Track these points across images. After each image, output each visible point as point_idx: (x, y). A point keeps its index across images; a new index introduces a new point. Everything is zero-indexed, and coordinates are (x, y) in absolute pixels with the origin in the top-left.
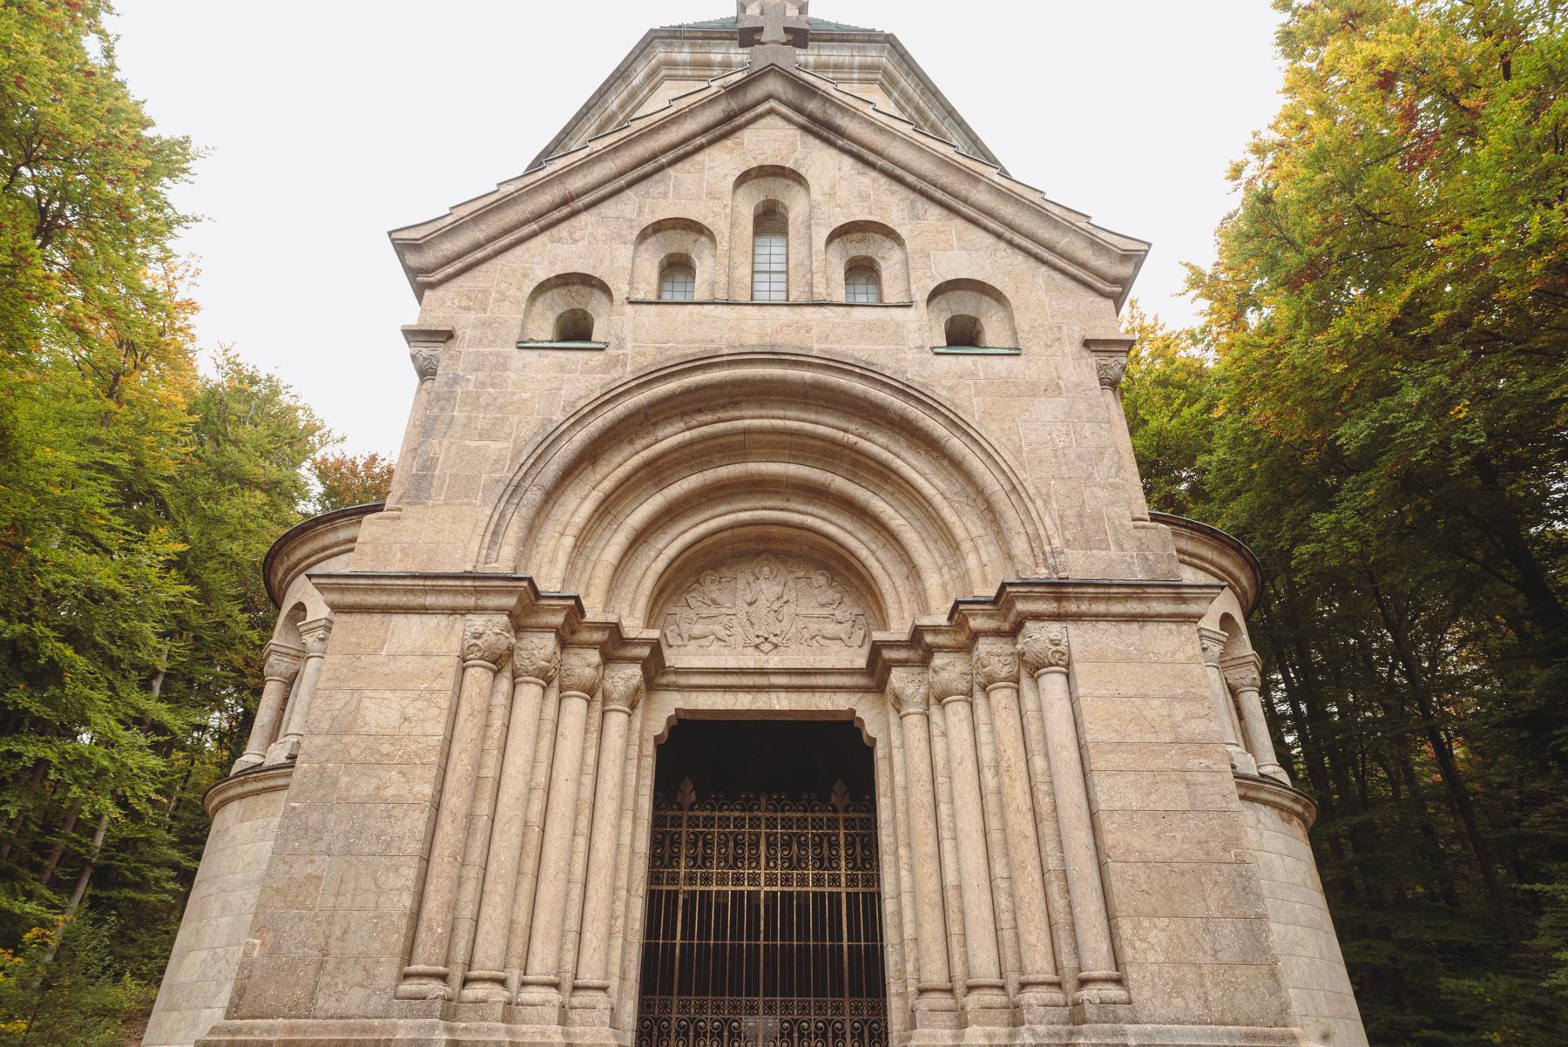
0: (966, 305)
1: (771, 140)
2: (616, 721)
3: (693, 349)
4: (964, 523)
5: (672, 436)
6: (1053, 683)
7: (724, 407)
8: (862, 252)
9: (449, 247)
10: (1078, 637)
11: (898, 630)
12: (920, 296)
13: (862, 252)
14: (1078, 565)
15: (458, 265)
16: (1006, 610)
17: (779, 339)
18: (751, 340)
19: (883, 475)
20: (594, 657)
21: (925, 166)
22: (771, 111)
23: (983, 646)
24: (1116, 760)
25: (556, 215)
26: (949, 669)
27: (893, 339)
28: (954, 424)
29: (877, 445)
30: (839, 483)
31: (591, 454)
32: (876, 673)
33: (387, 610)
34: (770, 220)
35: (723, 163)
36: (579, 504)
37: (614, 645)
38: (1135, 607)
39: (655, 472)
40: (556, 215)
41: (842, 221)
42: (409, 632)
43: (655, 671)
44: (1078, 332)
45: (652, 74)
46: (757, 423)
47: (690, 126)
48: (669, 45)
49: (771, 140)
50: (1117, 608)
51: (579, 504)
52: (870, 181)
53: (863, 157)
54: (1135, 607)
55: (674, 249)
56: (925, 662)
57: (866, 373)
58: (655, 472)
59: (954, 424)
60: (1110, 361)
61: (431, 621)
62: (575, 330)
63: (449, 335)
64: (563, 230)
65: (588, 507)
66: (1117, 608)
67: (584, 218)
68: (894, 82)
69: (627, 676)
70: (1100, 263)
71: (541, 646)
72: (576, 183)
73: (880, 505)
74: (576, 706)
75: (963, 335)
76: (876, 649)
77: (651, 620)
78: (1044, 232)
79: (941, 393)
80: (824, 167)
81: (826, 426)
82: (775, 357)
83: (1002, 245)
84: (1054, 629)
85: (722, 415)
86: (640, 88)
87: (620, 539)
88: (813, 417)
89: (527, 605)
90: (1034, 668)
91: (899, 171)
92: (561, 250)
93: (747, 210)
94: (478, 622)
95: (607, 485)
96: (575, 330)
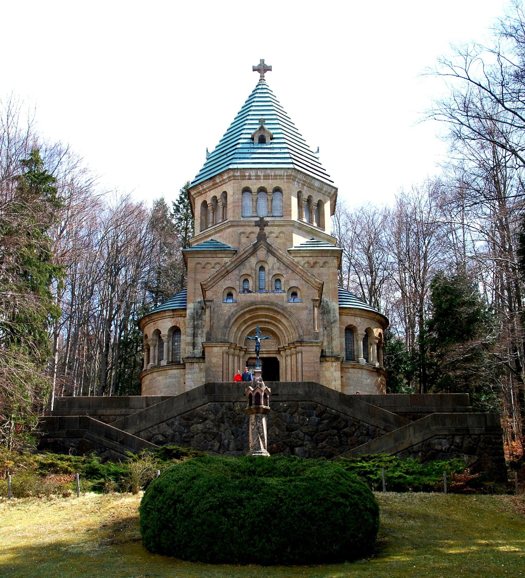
0: (295, 290)
2: (241, 359)
4: (291, 330)
5: (248, 316)
6: (300, 354)
9: (209, 284)
11: (282, 346)
12: (286, 290)
19: (280, 322)
20: (238, 351)
21: (289, 263)
23: (292, 349)
24: (306, 365)
26: (288, 352)
29: (279, 317)
30: (273, 322)
31: (236, 321)
32: (279, 352)
33: (212, 347)
34: (262, 268)
35: (253, 261)
36: (235, 329)
37: (241, 349)
38: (311, 344)
39: (245, 322)
41: (274, 274)
42: (216, 349)
44: (311, 297)
45: (229, 177)
47: (247, 254)
49: (262, 253)
51: (235, 329)
53: (279, 259)
54: (311, 344)
55: (246, 278)
56: (285, 350)
58: (245, 322)
61: (218, 348)
64: (227, 278)
65: (236, 329)
68: (296, 178)
69: (242, 353)
72: (228, 269)
73: (280, 326)
74: (236, 358)
76: (279, 348)
77: (245, 345)
78: (308, 278)
80: (271, 260)
82: (263, 302)
84: (300, 348)
87: (240, 332)
92: (227, 282)
93: (258, 269)
94: (224, 348)
95: (238, 325)
96: (230, 295)
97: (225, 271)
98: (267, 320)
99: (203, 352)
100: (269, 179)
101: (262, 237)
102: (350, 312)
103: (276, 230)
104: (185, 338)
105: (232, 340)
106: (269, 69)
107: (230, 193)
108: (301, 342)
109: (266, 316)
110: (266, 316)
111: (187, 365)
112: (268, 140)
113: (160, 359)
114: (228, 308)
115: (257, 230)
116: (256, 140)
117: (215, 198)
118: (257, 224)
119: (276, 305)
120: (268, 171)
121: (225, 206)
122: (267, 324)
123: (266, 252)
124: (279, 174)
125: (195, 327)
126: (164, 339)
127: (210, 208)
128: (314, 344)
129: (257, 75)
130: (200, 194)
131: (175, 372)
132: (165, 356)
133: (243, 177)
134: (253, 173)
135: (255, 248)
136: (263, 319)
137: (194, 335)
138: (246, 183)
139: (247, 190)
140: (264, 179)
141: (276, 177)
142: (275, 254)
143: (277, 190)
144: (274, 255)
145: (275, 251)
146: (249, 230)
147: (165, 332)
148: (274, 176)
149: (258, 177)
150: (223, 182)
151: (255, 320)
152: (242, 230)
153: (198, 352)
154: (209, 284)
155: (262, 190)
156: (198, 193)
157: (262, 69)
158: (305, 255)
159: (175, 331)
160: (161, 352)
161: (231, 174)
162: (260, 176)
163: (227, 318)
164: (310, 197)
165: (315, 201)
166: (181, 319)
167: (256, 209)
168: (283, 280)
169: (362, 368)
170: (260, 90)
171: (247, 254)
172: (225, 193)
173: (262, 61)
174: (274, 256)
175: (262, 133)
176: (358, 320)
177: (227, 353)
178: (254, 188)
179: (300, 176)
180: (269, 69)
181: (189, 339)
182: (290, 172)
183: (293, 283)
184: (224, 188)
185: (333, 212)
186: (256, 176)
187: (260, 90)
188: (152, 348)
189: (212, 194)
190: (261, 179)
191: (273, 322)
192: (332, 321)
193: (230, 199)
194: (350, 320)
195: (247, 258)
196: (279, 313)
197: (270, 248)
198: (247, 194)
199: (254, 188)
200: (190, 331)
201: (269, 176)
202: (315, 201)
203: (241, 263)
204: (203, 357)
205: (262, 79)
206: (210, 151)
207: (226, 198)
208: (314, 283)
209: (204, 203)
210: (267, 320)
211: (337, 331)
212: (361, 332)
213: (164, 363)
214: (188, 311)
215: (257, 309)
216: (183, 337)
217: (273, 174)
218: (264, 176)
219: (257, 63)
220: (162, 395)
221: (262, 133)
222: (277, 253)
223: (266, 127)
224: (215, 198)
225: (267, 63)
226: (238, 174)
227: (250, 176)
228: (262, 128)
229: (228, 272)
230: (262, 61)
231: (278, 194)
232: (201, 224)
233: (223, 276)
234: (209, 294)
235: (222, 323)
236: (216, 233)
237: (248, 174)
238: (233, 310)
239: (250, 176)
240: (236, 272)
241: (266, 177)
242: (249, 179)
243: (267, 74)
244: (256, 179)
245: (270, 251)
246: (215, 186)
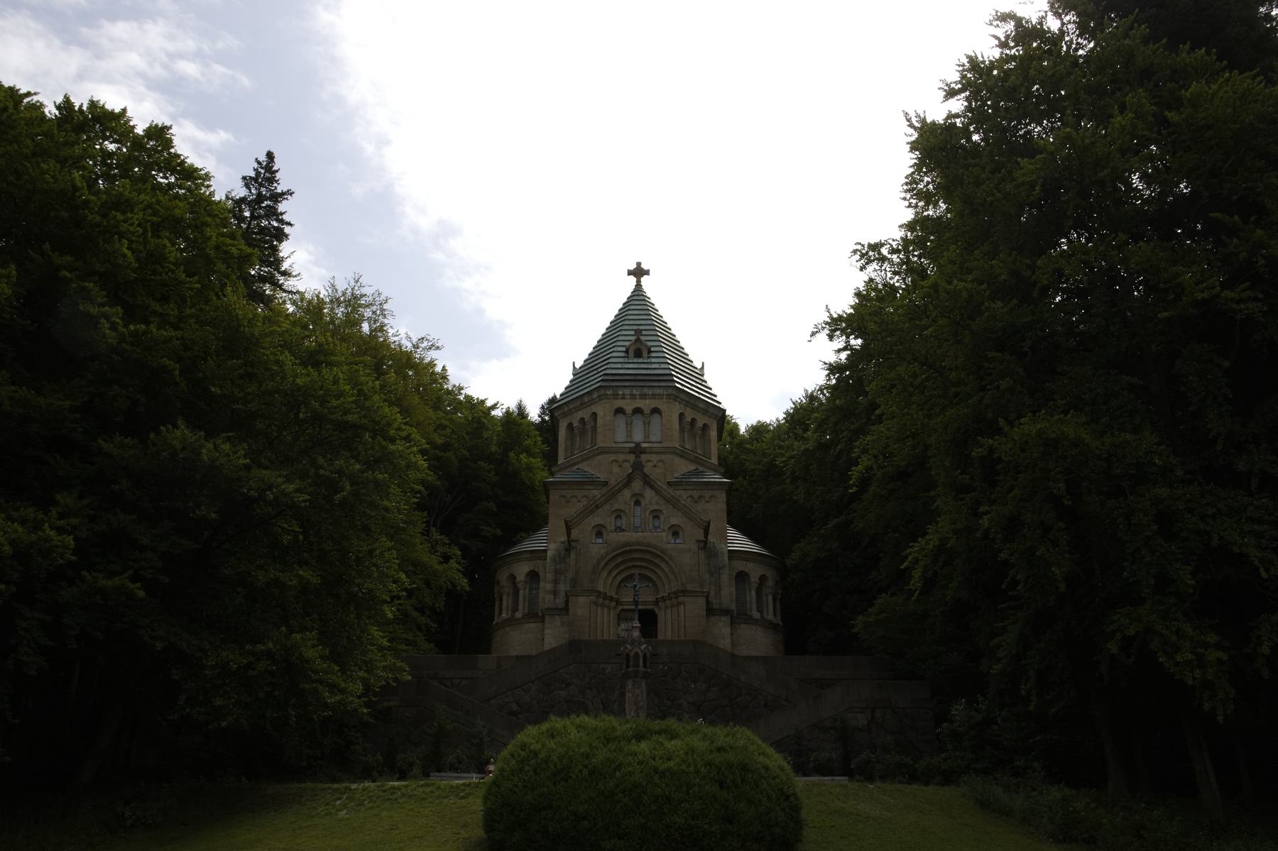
1: (637, 485)
5: (620, 560)
8: (656, 515)
10: (686, 599)
14: (689, 587)
16: (676, 594)
19: (658, 566)
26: (668, 602)
27: (662, 538)
29: (657, 561)
32: (657, 602)
34: (637, 503)
35: (627, 494)
36: (604, 574)
37: (611, 599)
39: (617, 566)
42: (581, 599)
43: (618, 602)
49: (637, 485)
51: (604, 574)
52: (656, 498)
58: (617, 566)
62: (599, 534)
71: (601, 600)
75: (675, 534)
80: (649, 493)
81: (647, 557)
82: (638, 544)
89: (599, 594)
90: (679, 604)
96: (599, 534)
99: (567, 602)
101: (638, 466)
103: (654, 458)
104: (546, 585)
105: (601, 589)
106: (647, 272)
107: (600, 414)
108: (684, 592)
109: (642, 560)
110: (642, 560)
111: (547, 618)
112: (645, 354)
113: (515, 609)
114: (596, 549)
115: (632, 458)
116: (631, 353)
117: (582, 419)
118: (632, 451)
119: (655, 547)
120: (646, 390)
121: (594, 429)
125: (556, 572)
126: (520, 585)
127: (576, 432)
129: (633, 280)
130: (565, 415)
131: (532, 626)
132: (521, 607)
133: (616, 396)
134: (627, 391)
135: (629, 479)
137: (556, 582)
138: (619, 403)
139: (620, 411)
141: (654, 396)
143: (656, 411)
144: (652, 487)
146: (621, 457)
147: (521, 577)
149: (633, 397)
150: (592, 402)
152: (613, 457)
153: (560, 601)
155: (638, 411)
157: (639, 272)
159: (534, 576)
160: (516, 602)
161: (602, 392)
164: (693, 420)
165: (700, 424)
166: (539, 562)
167: (629, 434)
168: (662, 517)
169: (755, 622)
170: (637, 300)
172: (594, 414)
173: (639, 264)
175: (638, 345)
177: (595, 603)
178: (629, 410)
179: (681, 396)
180: (647, 272)
181: (549, 586)
183: (674, 521)
184: (594, 408)
187: (637, 300)
188: (505, 597)
189: (580, 414)
193: (600, 421)
194: (740, 566)
195: (619, 490)
196: (658, 556)
198: (620, 416)
199: (629, 410)
200: (550, 576)
202: (700, 424)
203: (613, 495)
204: (565, 609)
205: (639, 285)
206: (578, 366)
207: (595, 420)
209: (570, 425)
211: (725, 578)
212: (754, 578)
213: (519, 615)
214: (549, 553)
215: (631, 551)
216: (542, 584)
219: (633, 267)
220: (515, 653)
221: (638, 345)
223: (643, 338)
224: (582, 419)
225: (644, 266)
226: (610, 392)
228: (638, 340)
229: (597, 507)
230: (639, 264)
231: (656, 417)
232: (566, 450)
233: (592, 512)
234: (575, 533)
236: (583, 460)
238: (603, 551)
240: (607, 507)
241: (643, 396)
243: (644, 280)
245: (648, 482)
246: (583, 406)
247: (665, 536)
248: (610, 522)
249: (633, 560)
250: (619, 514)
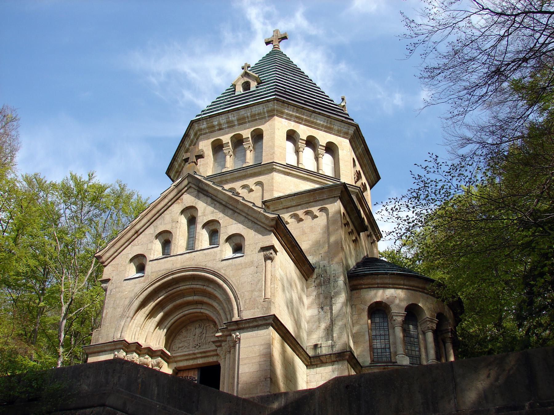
0: (237, 240)
3: (164, 272)
7: (175, 284)
9: (108, 255)
13: (213, 229)
15: (111, 259)
17: (185, 264)
18: (178, 266)
21: (226, 199)
22: (190, 187)
25: (134, 237)
28: (225, 281)
30: (206, 300)
31: (143, 305)
35: (177, 208)
40: (134, 237)
41: (205, 221)
46: (185, 287)
47: (166, 200)
48: (199, 123)
50: (251, 325)
55: (166, 238)
57: (203, 270)
59: (225, 281)
60: (268, 252)
63: (109, 280)
66: (251, 325)
67: (141, 236)
70: (267, 222)
72: (138, 227)
73: (215, 304)
78: (254, 215)
79: (222, 272)
83: (246, 220)
85: (174, 287)
86: (193, 139)
88: (196, 283)
91: (221, 201)
92: (135, 248)
96: (141, 268)
97: (133, 231)
98: (196, 298)
100: (245, 123)
102: (374, 281)
109: (195, 292)
110: (195, 292)
120: (242, 112)
122: (199, 306)
123: (196, 192)
124: (256, 112)
128: (260, 323)
136: (190, 298)
140: (239, 124)
142: (207, 192)
145: (206, 188)
148: (252, 116)
149: (231, 125)
151: (179, 302)
154: (108, 255)
156: (177, 172)
158: (289, 204)
162: (232, 121)
163: (127, 302)
171: (166, 200)
174: (207, 196)
176: (389, 293)
182: (270, 105)
185: (353, 159)
186: (228, 122)
190: (234, 125)
191: (206, 300)
192: (333, 294)
195: (167, 207)
197: (200, 185)
201: (244, 118)
208: (263, 220)
210: (196, 298)
217: (249, 114)
218: (238, 120)
222: (210, 190)
226: (204, 125)
227: (220, 124)
233: (130, 241)
235: (120, 310)
237: (216, 123)
239: (220, 124)
241: (242, 122)
242: (220, 129)
244: (229, 127)
247: (227, 251)
248: (156, 249)
249: (182, 294)
250: (166, 240)
